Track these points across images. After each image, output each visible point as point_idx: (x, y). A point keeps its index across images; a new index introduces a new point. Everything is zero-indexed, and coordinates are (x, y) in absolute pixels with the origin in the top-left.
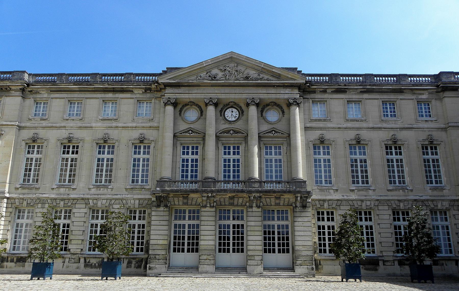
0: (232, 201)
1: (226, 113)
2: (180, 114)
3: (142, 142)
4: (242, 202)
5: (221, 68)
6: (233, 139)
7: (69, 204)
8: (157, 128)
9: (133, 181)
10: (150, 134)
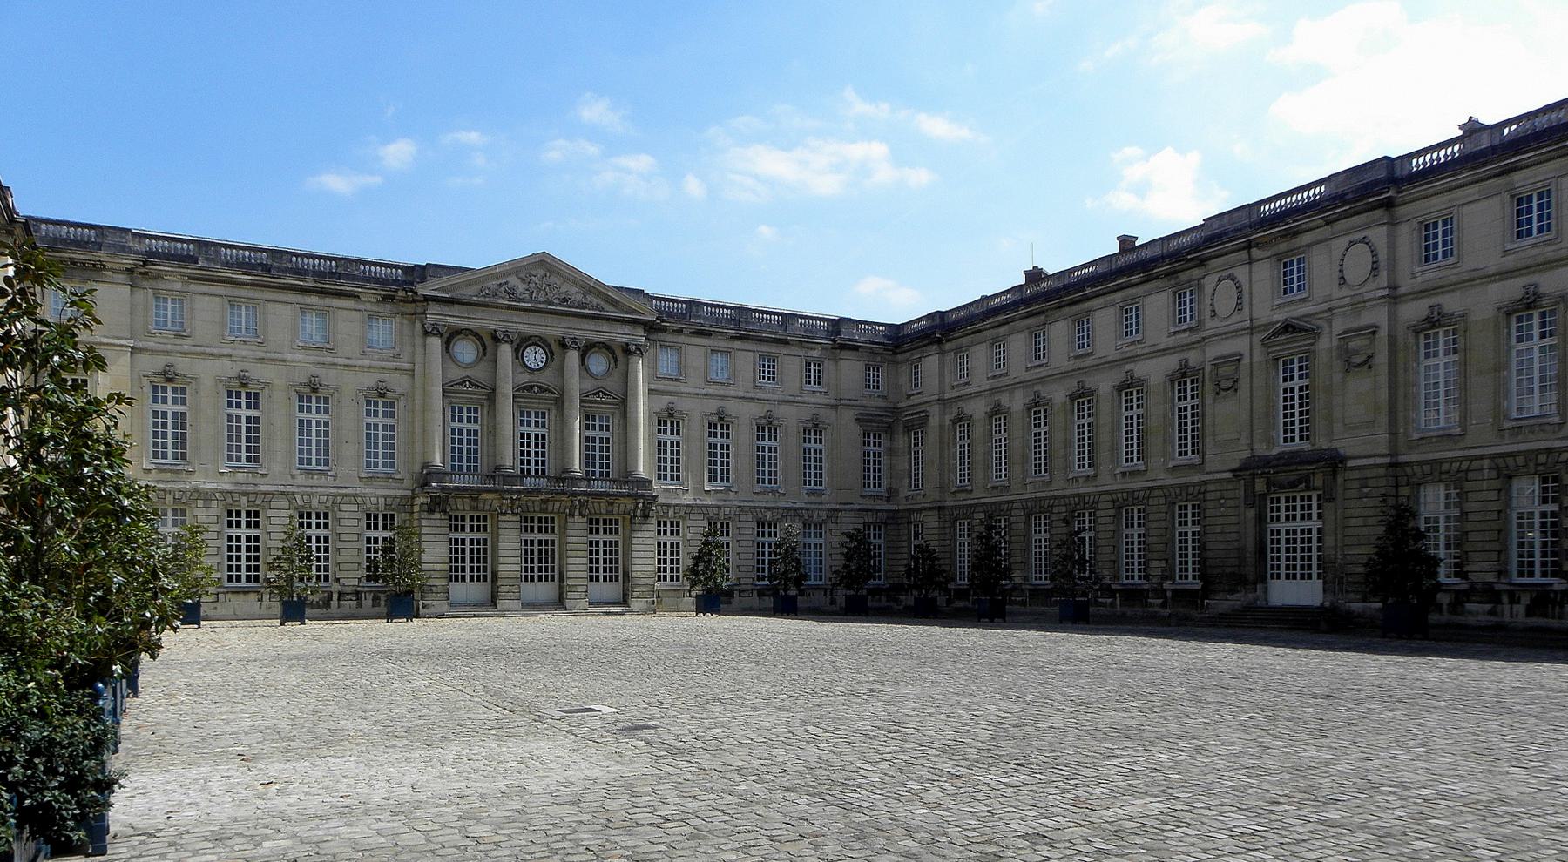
3: (382, 395)
5: (523, 276)
7: (258, 502)
8: (411, 373)
9: (368, 465)
10: (399, 383)
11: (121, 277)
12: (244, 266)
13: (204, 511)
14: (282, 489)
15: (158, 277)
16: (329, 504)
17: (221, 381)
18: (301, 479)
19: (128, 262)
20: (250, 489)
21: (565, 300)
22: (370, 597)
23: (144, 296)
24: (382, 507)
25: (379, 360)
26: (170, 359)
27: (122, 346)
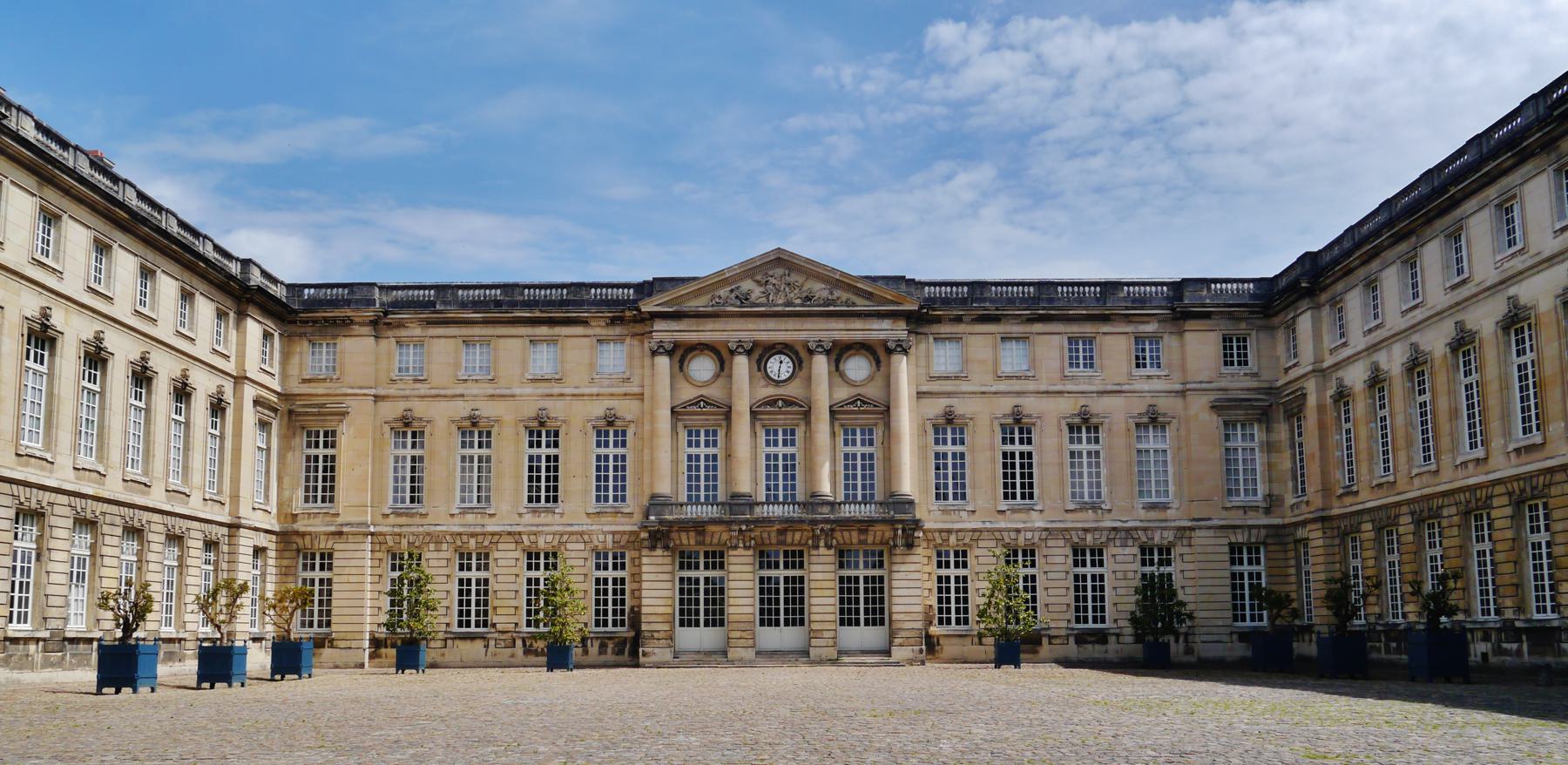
0: (782, 538)
1: (769, 365)
2: (681, 368)
3: (610, 424)
4: (801, 538)
5: (758, 278)
6: (782, 417)
7: (486, 543)
8: (640, 396)
10: (627, 409)
11: (366, 330)
12: (476, 305)
13: (435, 555)
14: (509, 529)
15: (400, 325)
16: (555, 543)
17: (453, 421)
18: (528, 518)
19: (369, 314)
20: (478, 529)
21: (808, 298)
22: (597, 644)
23: (388, 344)
24: (610, 544)
25: (608, 386)
26: (408, 405)
27: (365, 395)
